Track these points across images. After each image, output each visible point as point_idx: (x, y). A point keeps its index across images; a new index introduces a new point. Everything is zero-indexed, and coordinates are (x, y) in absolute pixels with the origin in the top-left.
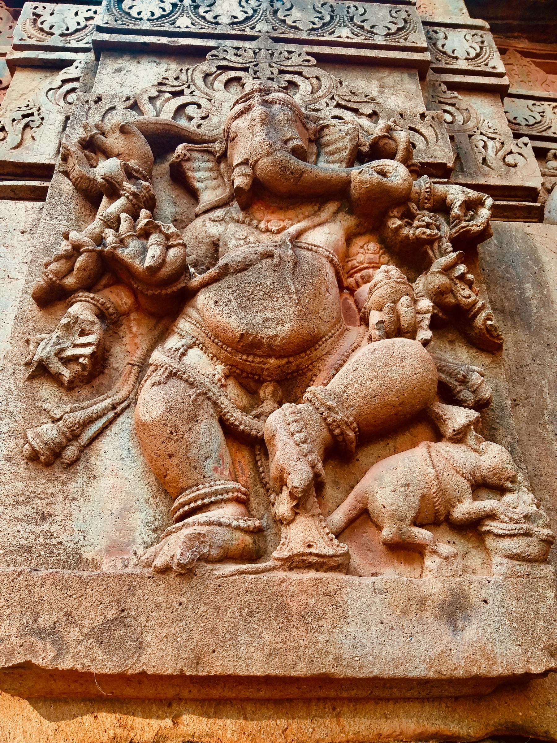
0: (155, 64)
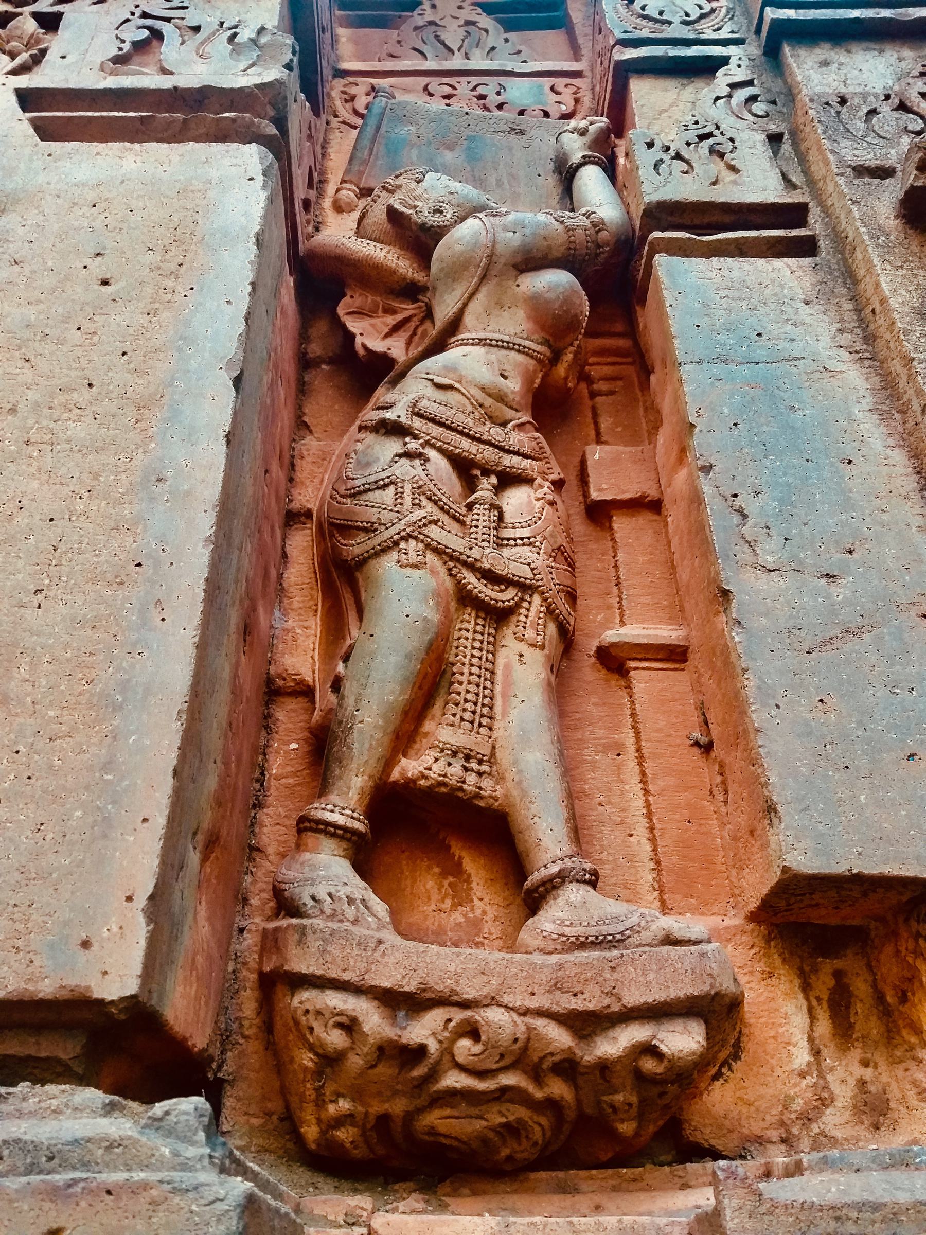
0: (876, 53)
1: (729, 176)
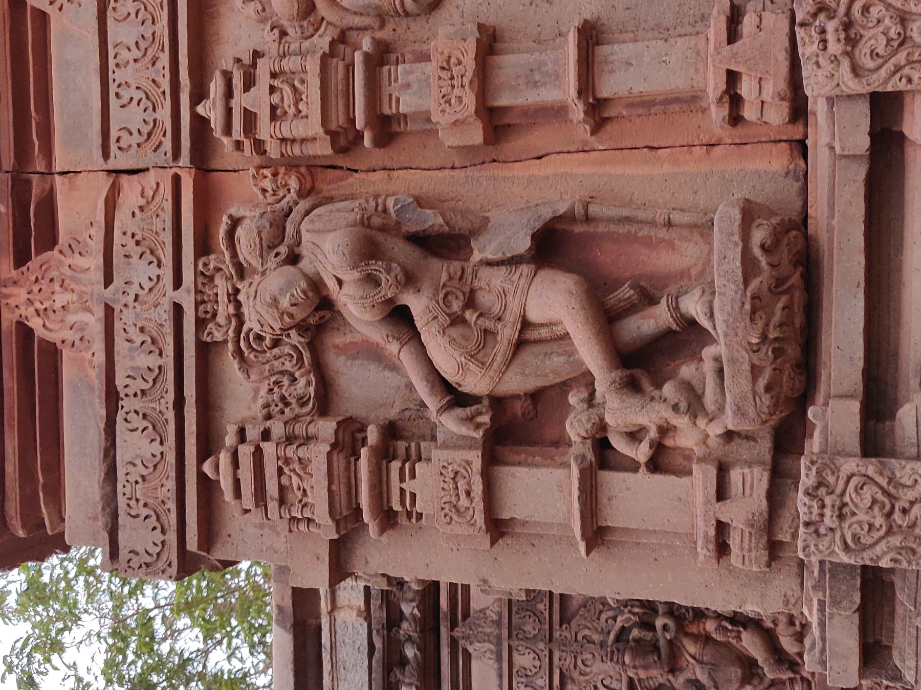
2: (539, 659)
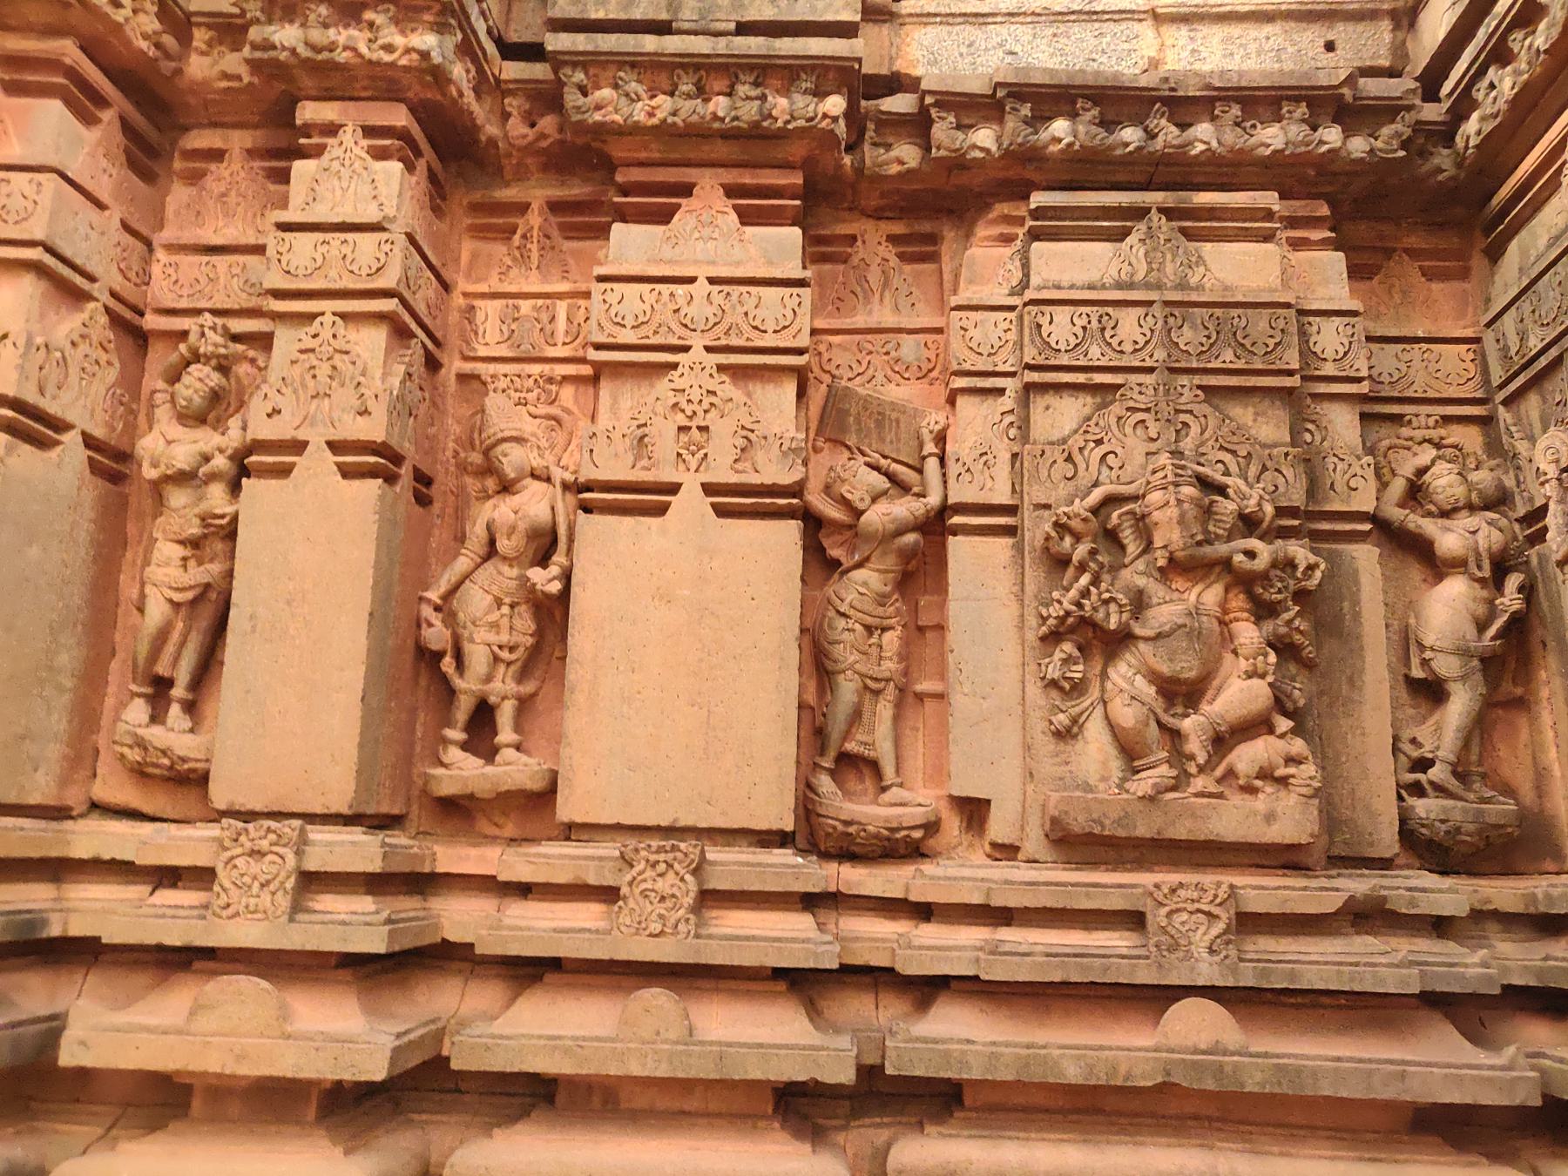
1: (989, 484)
2: (1136, 351)
